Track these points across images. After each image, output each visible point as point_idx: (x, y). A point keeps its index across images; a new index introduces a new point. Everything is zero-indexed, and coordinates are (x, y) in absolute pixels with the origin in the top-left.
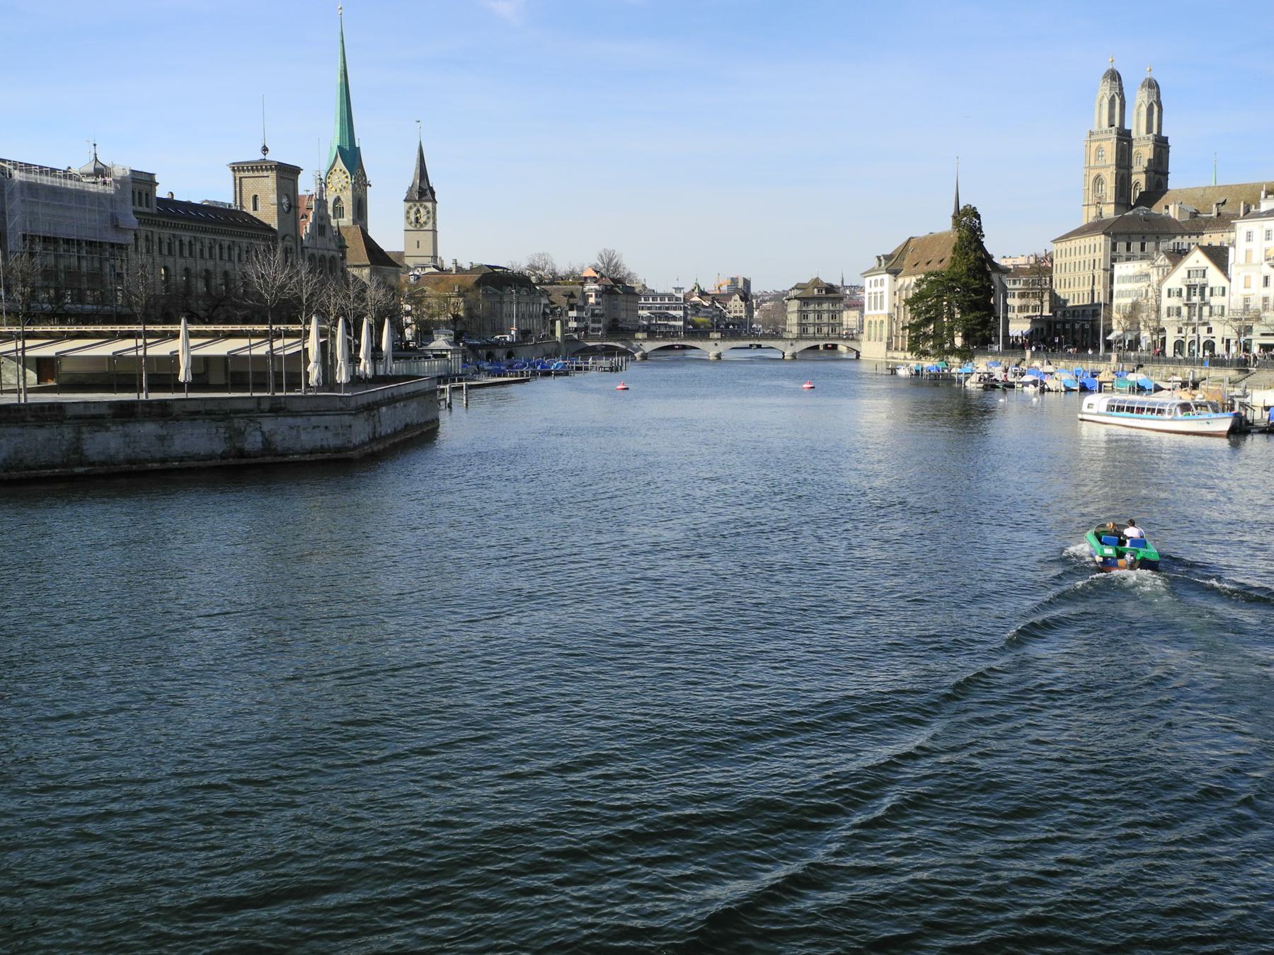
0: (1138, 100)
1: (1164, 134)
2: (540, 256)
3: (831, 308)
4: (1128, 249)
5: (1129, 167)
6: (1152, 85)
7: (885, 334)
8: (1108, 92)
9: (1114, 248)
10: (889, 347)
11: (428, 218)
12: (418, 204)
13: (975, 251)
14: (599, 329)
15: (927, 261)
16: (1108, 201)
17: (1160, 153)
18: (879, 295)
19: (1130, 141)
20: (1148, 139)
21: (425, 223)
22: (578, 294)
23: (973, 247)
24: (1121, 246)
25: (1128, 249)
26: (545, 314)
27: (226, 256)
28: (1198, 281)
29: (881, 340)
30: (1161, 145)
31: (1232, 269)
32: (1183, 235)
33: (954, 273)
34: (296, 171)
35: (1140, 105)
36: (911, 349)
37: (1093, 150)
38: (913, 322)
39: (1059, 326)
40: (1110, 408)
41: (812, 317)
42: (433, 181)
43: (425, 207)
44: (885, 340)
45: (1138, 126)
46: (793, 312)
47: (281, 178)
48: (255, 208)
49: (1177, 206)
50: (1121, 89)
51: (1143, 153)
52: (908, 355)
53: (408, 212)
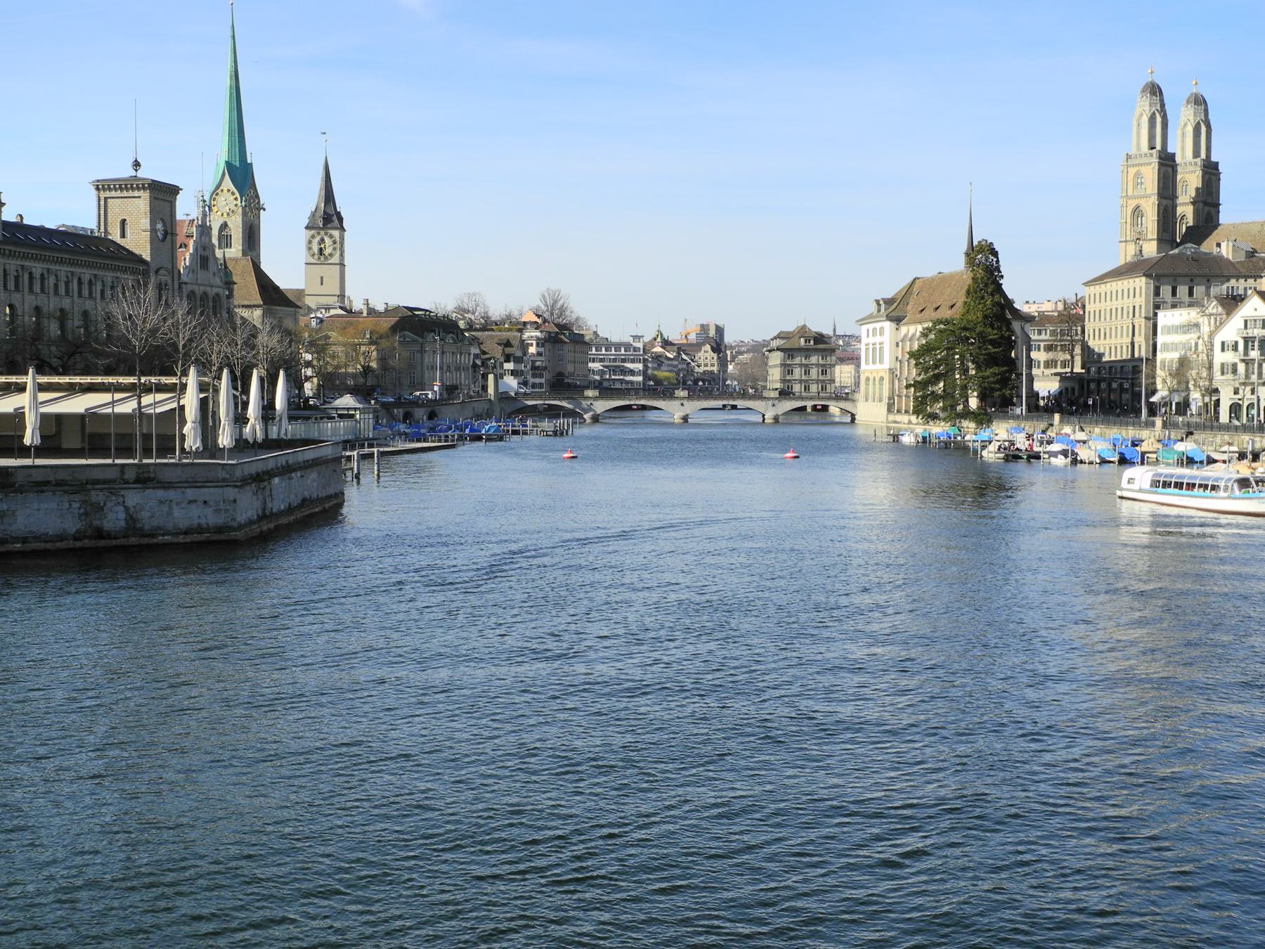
0: (1183, 119)
1: (1214, 159)
2: (469, 296)
3: (821, 362)
4: (1174, 293)
5: (1174, 197)
6: (1199, 101)
7: (886, 394)
8: (1147, 108)
9: (1157, 293)
10: (890, 410)
11: (334, 249)
12: (322, 232)
13: (992, 294)
14: (541, 385)
16: (1150, 236)
18: (878, 346)
20: (1196, 164)
21: (331, 255)
22: (515, 343)
23: (990, 290)
24: (1166, 290)
25: (1174, 293)
26: (475, 366)
27: (86, 292)
29: (881, 400)
30: (1211, 172)
32: (1238, 278)
33: (968, 321)
34: (173, 191)
35: (1186, 125)
36: (917, 412)
38: (919, 379)
39: (1093, 386)
40: (1155, 483)
41: (797, 373)
42: (341, 205)
43: (331, 236)
44: (886, 400)
45: (1183, 149)
46: (775, 366)
47: (155, 198)
48: (123, 235)
49: (1231, 244)
50: (1163, 105)
51: (1190, 180)
52: (913, 418)
53: (310, 242)
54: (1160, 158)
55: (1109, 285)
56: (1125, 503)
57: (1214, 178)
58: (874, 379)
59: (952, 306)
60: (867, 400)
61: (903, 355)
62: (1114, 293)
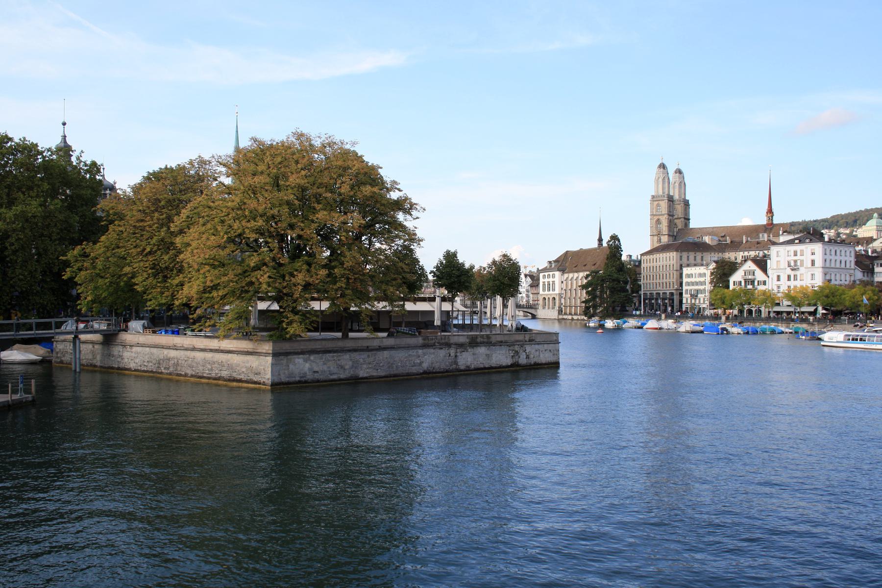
1: (687, 198)
6: (679, 172)
10: (560, 312)
16: (664, 233)
28: (750, 277)
31: (769, 272)
37: (655, 206)
40: (847, 339)
44: (557, 308)
45: (674, 193)
54: (668, 197)
55: (655, 255)
56: (826, 349)
57: (687, 207)
59: (595, 265)
60: (544, 308)
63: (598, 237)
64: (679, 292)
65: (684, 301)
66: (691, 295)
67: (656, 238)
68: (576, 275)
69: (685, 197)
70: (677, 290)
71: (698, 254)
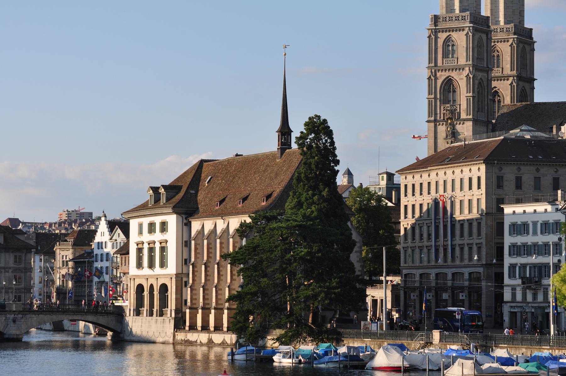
1: (527, 25)
10: (179, 324)
15: (244, 195)
17: (524, 49)
18: (158, 246)
19: (488, 33)
29: (161, 314)
55: (433, 174)
57: (528, 48)
58: (152, 286)
61: (196, 257)
62: (441, 183)
63: (277, 123)
64: (494, 270)
65: (507, 296)
66: (525, 280)
67: (442, 129)
68: (221, 225)
69: (522, 21)
70: (488, 266)
71: (544, 170)
